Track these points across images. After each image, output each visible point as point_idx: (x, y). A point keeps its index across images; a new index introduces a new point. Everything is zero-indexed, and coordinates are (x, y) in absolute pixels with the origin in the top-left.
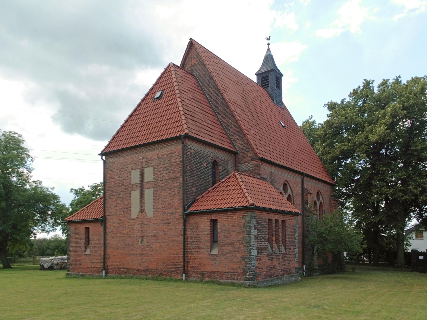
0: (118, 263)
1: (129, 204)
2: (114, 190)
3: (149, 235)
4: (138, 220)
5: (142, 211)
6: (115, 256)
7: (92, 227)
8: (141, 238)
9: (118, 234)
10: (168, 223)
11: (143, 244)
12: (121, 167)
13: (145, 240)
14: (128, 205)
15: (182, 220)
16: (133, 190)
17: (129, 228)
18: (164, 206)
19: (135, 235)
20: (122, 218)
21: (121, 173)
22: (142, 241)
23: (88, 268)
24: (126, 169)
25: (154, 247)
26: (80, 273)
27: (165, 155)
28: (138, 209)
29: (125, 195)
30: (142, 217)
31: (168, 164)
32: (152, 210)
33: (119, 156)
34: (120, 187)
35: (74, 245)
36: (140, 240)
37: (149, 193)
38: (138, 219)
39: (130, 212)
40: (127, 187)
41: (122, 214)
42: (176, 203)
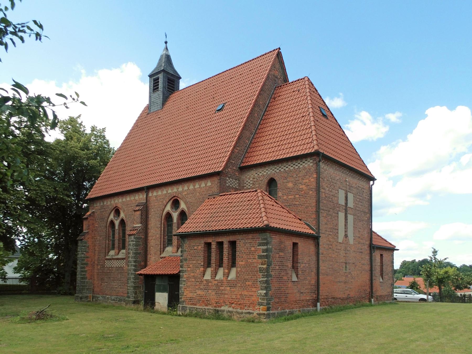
0: (327, 292)
1: (336, 225)
2: (324, 203)
3: (350, 262)
4: (343, 245)
5: (346, 236)
6: (324, 284)
7: (302, 243)
8: (345, 264)
9: (328, 258)
10: (361, 252)
11: (346, 271)
12: (330, 180)
13: (348, 266)
14: (336, 226)
15: (368, 251)
16: (340, 211)
17: (336, 252)
18: (359, 236)
19: (341, 261)
20: (331, 240)
21: (330, 186)
22: (346, 267)
23: (296, 301)
24: (335, 185)
25: (353, 274)
26: (288, 311)
27: (360, 187)
28: (344, 234)
29: (334, 214)
30: (346, 242)
31: (361, 197)
32: (353, 238)
33: (329, 166)
34: (330, 203)
35: (277, 268)
36: (344, 266)
37: (351, 218)
38: (343, 243)
39: (337, 234)
40: (335, 204)
41: (331, 235)
42: (366, 235)
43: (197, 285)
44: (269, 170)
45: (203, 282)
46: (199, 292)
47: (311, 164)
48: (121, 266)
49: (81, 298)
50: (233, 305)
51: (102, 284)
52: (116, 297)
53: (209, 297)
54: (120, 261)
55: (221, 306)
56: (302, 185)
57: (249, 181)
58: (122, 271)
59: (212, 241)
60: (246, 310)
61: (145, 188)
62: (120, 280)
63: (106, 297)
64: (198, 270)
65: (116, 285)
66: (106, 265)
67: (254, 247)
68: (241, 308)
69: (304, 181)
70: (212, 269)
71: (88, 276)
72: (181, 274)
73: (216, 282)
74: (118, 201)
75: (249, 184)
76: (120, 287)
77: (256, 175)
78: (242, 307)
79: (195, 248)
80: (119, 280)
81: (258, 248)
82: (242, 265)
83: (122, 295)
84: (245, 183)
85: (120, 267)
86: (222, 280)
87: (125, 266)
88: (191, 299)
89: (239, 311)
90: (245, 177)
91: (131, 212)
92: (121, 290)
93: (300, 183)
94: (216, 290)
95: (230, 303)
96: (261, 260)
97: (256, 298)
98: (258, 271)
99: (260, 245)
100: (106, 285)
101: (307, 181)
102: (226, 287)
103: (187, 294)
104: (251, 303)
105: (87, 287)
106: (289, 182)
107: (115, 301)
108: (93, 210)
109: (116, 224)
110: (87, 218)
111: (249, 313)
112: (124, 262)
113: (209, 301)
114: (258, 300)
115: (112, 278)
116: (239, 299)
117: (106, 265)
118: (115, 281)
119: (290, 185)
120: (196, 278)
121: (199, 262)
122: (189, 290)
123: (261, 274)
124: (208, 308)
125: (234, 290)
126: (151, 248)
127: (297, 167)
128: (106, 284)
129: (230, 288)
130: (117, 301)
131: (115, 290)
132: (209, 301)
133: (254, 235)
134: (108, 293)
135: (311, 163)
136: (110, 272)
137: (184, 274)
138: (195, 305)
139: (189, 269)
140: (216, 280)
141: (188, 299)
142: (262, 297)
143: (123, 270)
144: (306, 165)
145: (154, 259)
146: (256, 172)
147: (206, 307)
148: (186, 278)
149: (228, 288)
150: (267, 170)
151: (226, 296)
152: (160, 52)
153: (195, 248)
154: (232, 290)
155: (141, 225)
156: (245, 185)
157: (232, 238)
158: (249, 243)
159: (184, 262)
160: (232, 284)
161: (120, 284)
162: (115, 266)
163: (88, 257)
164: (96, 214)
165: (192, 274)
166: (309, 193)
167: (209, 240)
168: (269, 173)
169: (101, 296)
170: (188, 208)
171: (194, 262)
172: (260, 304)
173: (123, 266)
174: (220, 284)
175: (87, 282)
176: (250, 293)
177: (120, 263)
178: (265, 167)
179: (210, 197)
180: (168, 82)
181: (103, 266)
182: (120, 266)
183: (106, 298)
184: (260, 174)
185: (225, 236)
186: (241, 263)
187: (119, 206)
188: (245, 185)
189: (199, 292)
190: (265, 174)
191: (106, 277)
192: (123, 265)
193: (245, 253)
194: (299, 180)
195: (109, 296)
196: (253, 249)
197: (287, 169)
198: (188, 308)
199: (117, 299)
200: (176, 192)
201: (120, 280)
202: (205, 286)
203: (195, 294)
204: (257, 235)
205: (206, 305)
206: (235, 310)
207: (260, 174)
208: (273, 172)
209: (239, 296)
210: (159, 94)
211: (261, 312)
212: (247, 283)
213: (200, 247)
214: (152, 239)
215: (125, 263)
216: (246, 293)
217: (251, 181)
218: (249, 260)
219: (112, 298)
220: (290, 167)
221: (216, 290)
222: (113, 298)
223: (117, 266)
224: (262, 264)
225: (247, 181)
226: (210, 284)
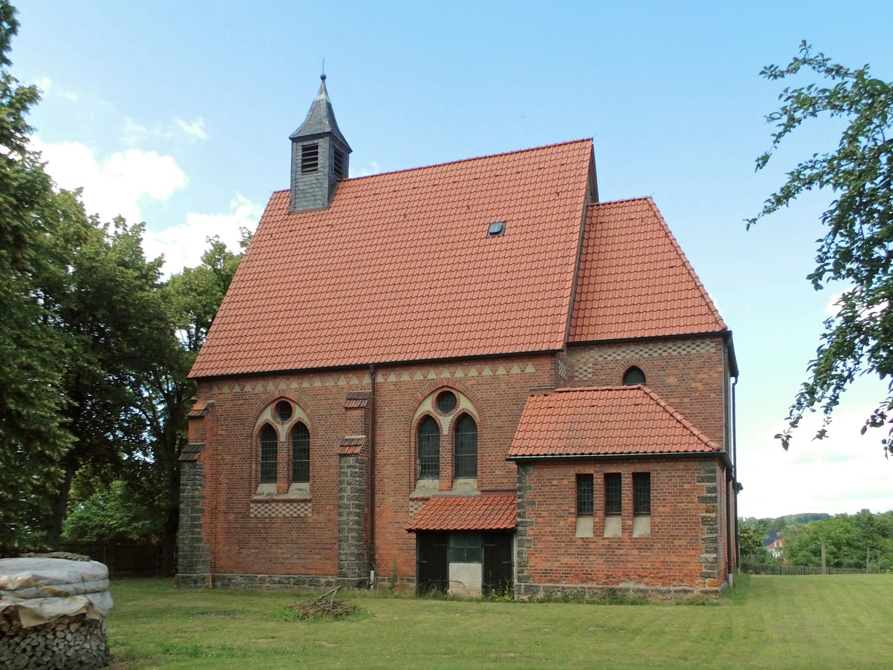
43: (560, 548)
44: (628, 351)
45: (575, 542)
46: (565, 560)
47: (713, 350)
48: (298, 515)
49: (195, 582)
50: (646, 580)
51: (242, 550)
52: (287, 576)
53: (589, 568)
55: (618, 583)
56: (696, 382)
57: (585, 368)
58: (303, 525)
59: (595, 472)
60: (674, 586)
61: (371, 367)
64: (562, 523)
65: (284, 553)
66: (252, 513)
67: (688, 483)
68: (664, 584)
69: (700, 376)
70: (597, 520)
71: (204, 535)
72: (520, 528)
73: (606, 542)
74: (289, 388)
75: (585, 373)
76: (296, 556)
77: (601, 359)
78: (667, 581)
79: (555, 482)
81: (699, 486)
82: (664, 513)
83: (303, 572)
84: (577, 371)
85: (295, 517)
86: (619, 538)
88: (546, 572)
89: (662, 588)
90: (575, 361)
93: (692, 379)
94: (606, 555)
95: (639, 576)
96: (704, 504)
97: (697, 566)
98: (699, 523)
99: (702, 480)
100: (253, 553)
101: (706, 376)
102: (628, 549)
103: (536, 563)
104: (686, 575)
105: (203, 559)
106: (670, 375)
108: (211, 401)
109: (281, 433)
110: (200, 418)
111: (685, 591)
112: (306, 507)
113: (591, 574)
114: (700, 570)
116: (660, 569)
117: (252, 513)
119: (672, 380)
120: (559, 535)
121: (565, 507)
122: (541, 557)
123: (706, 527)
124: (589, 586)
125: (648, 554)
126: (385, 480)
127: (684, 353)
128: (252, 551)
129: (639, 552)
132: (591, 574)
133: (689, 464)
135: (712, 347)
137: (528, 528)
138: (557, 582)
139: (540, 520)
140: (605, 539)
141: (539, 573)
142: (708, 564)
144: (703, 351)
145: (394, 501)
146: (601, 354)
147: (584, 585)
148: (532, 536)
149: (635, 552)
150: (623, 352)
151: (630, 565)
152: (314, 95)
153: (555, 482)
154: (642, 554)
155: (365, 436)
156: (577, 374)
157: (640, 468)
158: (678, 476)
159: (528, 509)
160: (643, 545)
163: (204, 497)
164: (218, 408)
165: (548, 529)
166: (709, 396)
167: (588, 470)
168: (628, 357)
169: (241, 577)
170: (480, 410)
171: (552, 507)
172: (704, 576)
174: (615, 546)
175: (203, 548)
176: (684, 559)
178: (620, 347)
179: (533, 393)
180: (335, 158)
181: (246, 516)
182: (295, 515)
184: (610, 358)
185: (625, 465)
186: (661, 509)
187: (291, 395)
188: (577, 374)
189: (565, 560)
190: (619, 358)
192: (306, 512)
193: (669, 493)
194: (689, 374)
196: (687, 486)
197: (665, 354)
198: (541, 588)
200: (447, 379)
202: (579, 548)
203: (558, 564)
204: (695, 465)
205: (583, 582)
206: (652, 588)
207: (610, 358)
208: (637, 356)
209: (658, 565)
210: (319, 178)
211: (707, 588)
212: (676, 542)
213: (565, 482)
214: (386, 464)
215: (310, 510)
216: (675, 559)
217: (589, 368)
218: (679, 505)
220: (672, 351)
221: (606, 555)
222: (277, 579)
223: (288, 515)
224: (707, 512)
225: (580, 368)
226: (592, 545)
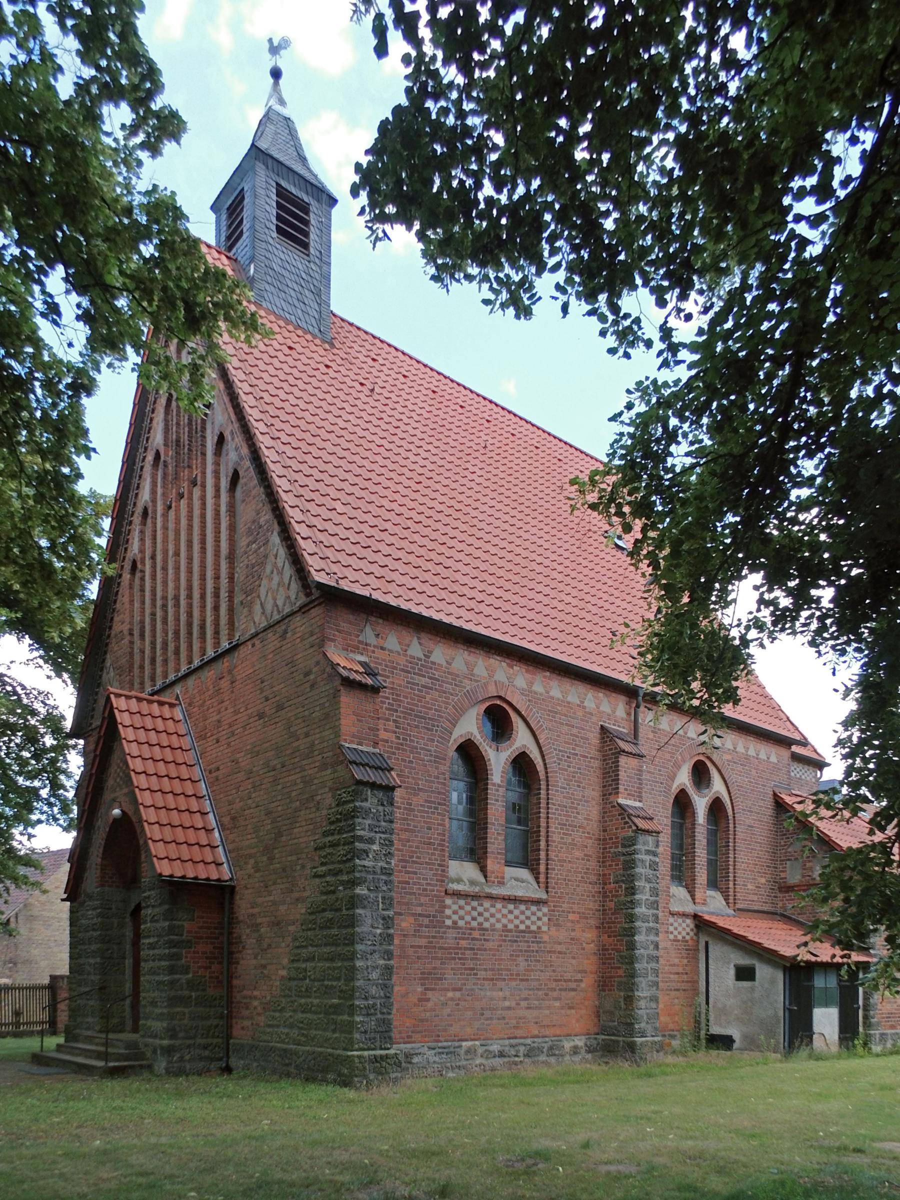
48: (527, 927)
51: (430, 994)
52: (512, 1041)
54: (523, 907)
58: (535, 947)
62: (527, 980)
63: (460, 1046)
65: (505, 999)
66: (449, 917)
76: (524, 1004)
80: (522, 980)
83: (536, 1032)
85: (523, 931)
87: (545, 928)
91: (566, 742)
92: (529, 1014)
100: (452, 999)
107: (506, 1060)
109: (494, 767)
112: (540, 914)
115: (486, 970)
117: (449, 917)
118: (501, 984)
128: (450, 994)
130: (516, 1056)
131: (504, 1018)
134: (468, 1030)
136: (472, 949)
143: (538, 942)
161: (525, 994)
162: (499, 926)
169: (430, 1048)
173: (539, 928)
177: (522, 917)
181: (436, 921)
182: (522, 927)
183: (462, 1052)
191: (452, 969)
192: (539, 923)
195: (477, 1043)
199: (518, 1051)
201: (527, 980)
203: (895, 1006)
215: (545, 919)
219: (491, 1048)
222: (495, 1048)
223: (511, 926)
